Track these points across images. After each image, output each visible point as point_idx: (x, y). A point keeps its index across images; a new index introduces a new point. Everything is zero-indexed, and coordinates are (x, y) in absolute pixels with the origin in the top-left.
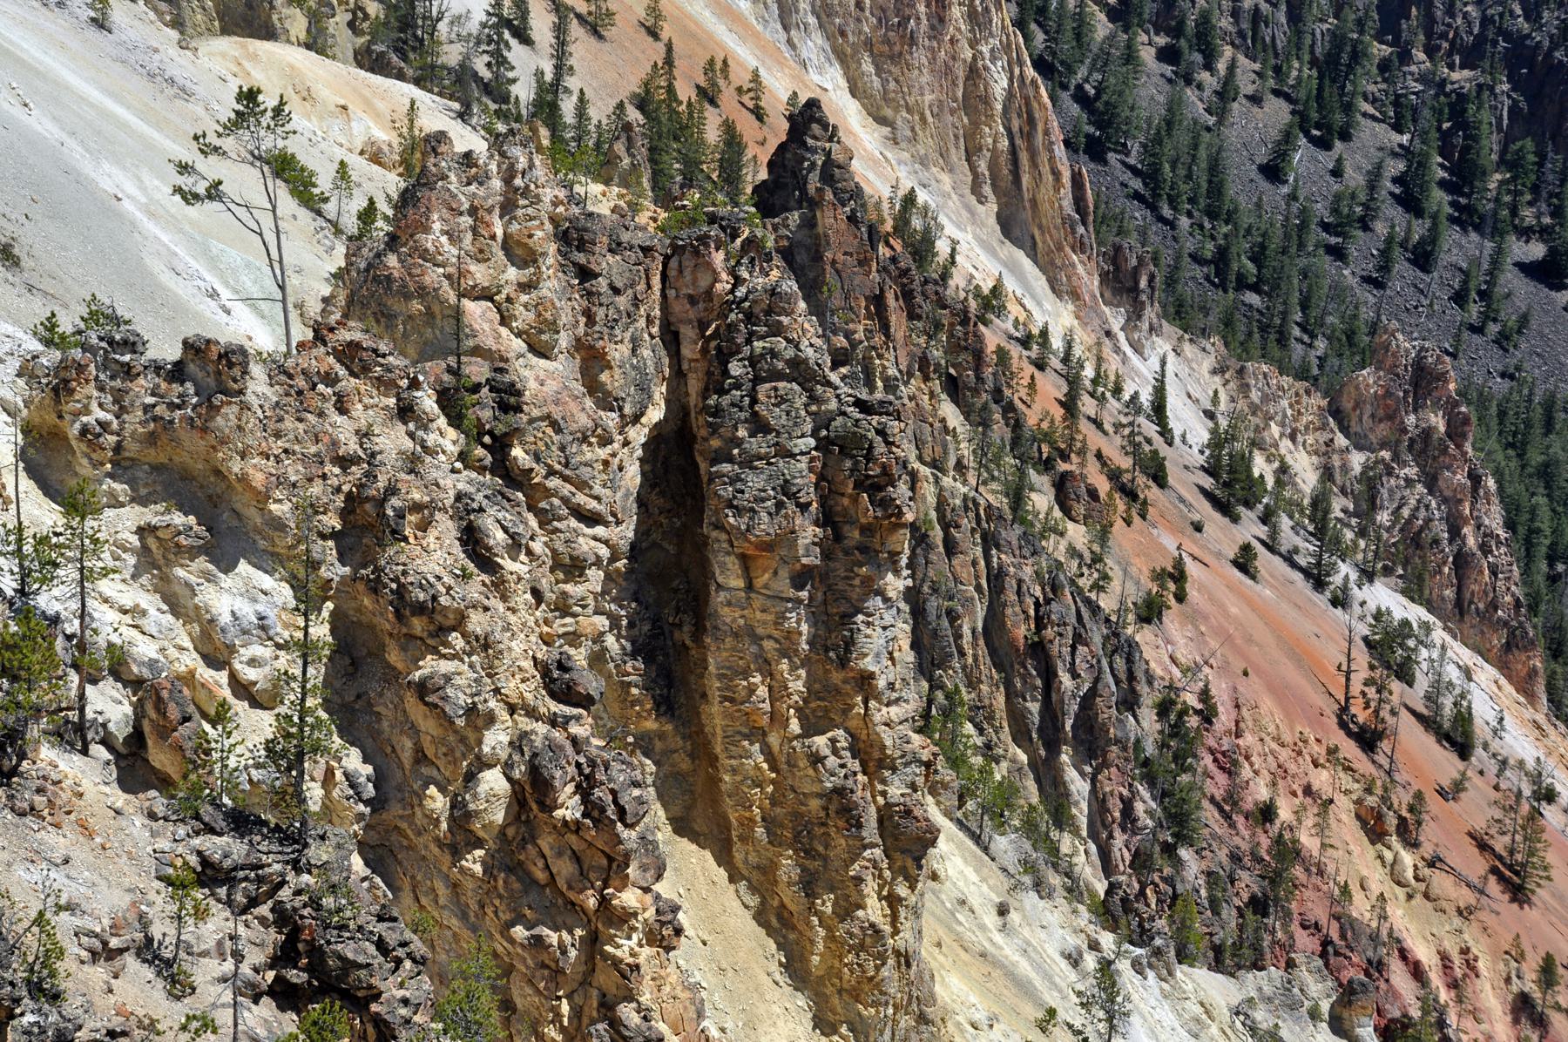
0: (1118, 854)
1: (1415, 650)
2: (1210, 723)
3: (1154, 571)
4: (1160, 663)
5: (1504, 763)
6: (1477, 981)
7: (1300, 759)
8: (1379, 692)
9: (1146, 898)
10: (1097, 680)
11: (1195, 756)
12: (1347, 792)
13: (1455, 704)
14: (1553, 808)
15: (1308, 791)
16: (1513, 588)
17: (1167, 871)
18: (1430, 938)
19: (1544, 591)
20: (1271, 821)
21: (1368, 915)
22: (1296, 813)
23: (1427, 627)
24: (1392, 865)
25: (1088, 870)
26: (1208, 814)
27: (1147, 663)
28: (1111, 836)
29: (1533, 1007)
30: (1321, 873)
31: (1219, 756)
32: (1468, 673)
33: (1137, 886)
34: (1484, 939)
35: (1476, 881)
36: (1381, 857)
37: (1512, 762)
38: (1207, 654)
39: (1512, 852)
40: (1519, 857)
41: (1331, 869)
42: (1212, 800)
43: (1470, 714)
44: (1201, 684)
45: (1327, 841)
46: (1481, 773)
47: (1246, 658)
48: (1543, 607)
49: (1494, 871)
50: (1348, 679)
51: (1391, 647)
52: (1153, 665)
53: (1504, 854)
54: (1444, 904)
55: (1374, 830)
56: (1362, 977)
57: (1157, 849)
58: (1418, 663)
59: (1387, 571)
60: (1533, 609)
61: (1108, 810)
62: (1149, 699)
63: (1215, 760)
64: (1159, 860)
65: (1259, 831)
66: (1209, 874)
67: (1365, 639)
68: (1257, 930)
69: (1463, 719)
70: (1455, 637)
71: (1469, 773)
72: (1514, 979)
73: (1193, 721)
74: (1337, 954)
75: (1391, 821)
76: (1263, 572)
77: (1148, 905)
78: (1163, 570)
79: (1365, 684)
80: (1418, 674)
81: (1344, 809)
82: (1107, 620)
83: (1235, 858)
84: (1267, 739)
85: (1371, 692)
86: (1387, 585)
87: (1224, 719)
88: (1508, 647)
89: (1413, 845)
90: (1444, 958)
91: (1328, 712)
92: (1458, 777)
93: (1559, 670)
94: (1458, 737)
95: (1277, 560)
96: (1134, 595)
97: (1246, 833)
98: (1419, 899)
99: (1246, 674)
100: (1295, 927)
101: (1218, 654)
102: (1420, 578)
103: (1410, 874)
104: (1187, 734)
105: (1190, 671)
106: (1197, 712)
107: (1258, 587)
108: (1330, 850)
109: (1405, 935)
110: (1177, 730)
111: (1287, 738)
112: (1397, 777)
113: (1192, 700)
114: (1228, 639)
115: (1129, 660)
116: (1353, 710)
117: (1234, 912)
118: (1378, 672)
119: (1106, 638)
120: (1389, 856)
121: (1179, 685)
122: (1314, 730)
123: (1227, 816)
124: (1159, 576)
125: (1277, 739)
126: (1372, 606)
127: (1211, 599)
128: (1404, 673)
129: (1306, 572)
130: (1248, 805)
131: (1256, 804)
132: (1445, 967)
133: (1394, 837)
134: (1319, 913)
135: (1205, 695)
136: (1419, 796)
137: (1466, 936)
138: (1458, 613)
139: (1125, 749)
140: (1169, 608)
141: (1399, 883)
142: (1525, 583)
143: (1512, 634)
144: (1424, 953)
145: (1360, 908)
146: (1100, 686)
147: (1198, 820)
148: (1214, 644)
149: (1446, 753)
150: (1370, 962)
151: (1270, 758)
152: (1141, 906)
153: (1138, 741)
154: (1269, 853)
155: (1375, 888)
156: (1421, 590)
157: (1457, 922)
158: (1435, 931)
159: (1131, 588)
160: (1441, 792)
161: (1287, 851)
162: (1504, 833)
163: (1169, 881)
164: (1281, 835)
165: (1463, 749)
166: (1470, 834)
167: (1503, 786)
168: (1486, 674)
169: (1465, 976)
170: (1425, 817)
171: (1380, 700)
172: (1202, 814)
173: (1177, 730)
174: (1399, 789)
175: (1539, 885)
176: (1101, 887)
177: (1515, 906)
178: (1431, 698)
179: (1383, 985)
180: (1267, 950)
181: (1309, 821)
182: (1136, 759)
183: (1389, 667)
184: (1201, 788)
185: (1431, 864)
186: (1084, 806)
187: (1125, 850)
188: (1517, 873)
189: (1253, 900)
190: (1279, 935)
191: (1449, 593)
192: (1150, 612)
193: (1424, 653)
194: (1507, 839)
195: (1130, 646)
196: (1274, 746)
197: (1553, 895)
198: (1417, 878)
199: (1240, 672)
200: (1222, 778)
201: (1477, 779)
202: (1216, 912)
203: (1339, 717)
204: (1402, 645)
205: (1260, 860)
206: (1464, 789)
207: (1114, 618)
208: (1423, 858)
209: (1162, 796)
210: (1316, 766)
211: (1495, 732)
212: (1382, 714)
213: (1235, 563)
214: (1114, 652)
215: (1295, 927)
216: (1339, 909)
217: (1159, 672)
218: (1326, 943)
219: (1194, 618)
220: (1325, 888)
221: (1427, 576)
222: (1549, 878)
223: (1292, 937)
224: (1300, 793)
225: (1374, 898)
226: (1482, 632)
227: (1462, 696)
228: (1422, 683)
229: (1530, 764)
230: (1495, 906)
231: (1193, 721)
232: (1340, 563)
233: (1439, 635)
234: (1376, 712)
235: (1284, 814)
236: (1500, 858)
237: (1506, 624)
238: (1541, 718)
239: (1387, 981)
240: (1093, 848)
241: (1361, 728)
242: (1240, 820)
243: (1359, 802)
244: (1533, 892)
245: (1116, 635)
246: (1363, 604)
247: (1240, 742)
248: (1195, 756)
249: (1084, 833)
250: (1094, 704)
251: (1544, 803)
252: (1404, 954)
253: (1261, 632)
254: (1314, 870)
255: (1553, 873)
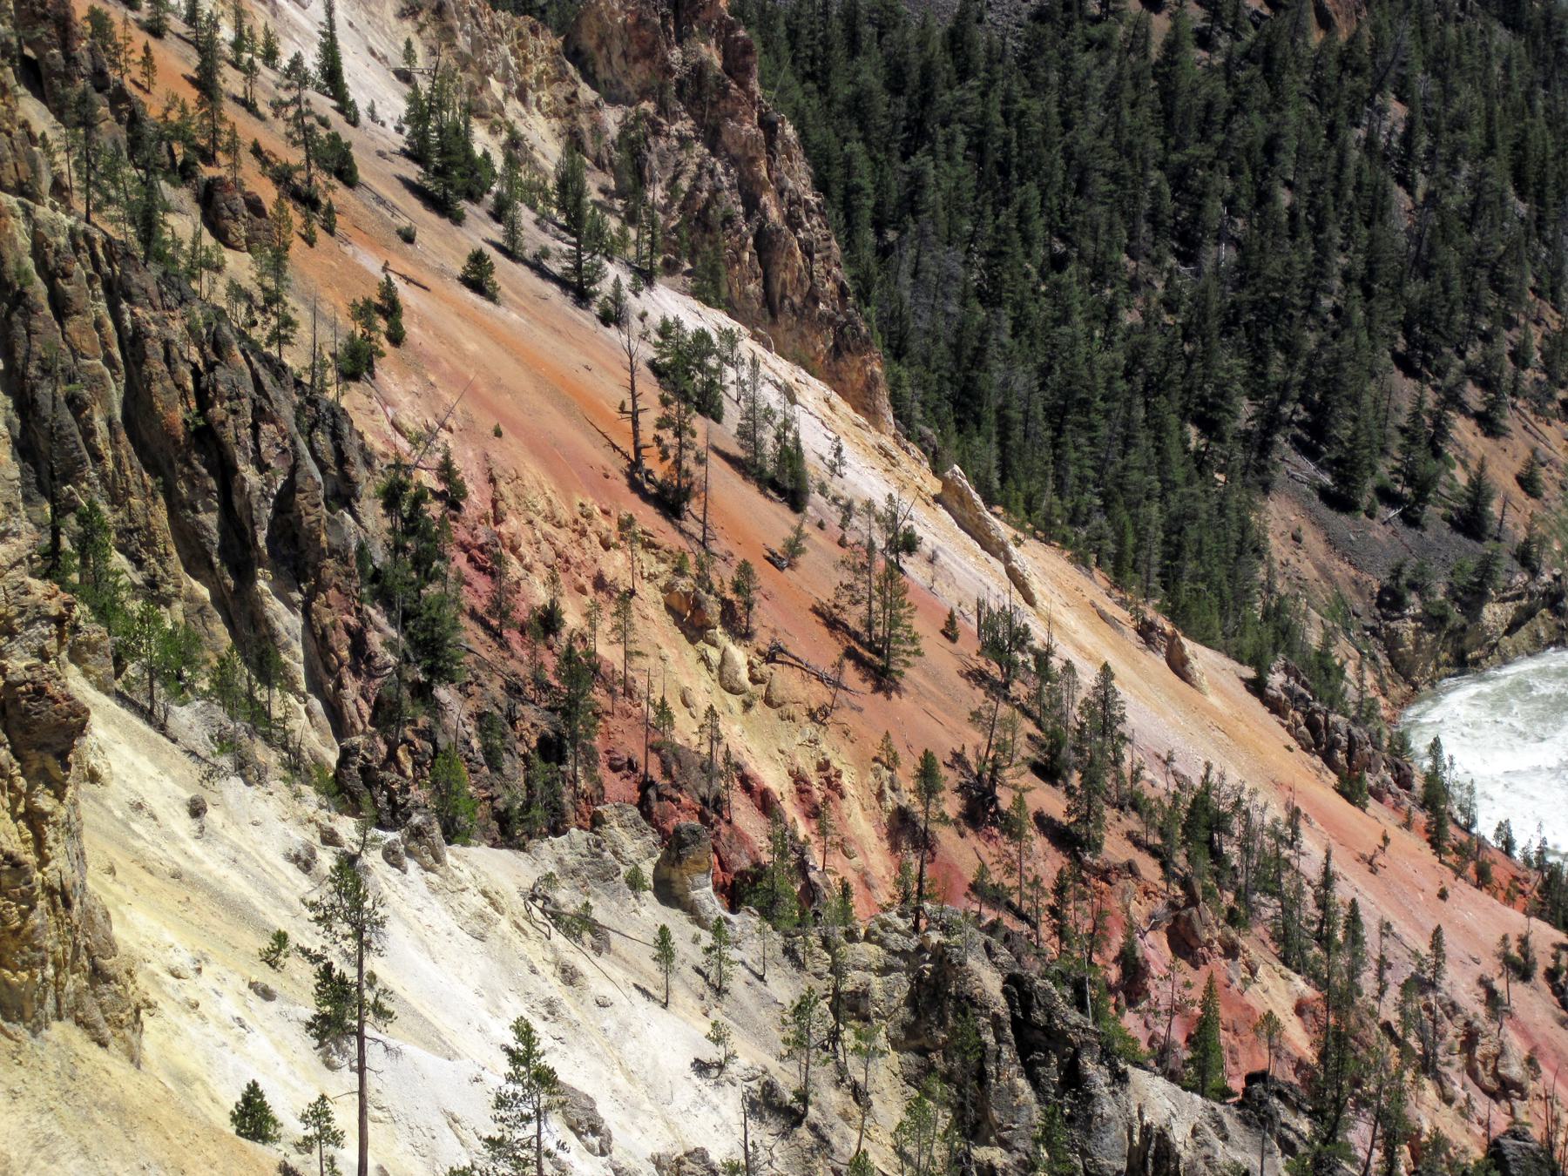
0: (353, 708)
1: (719, 371)
2: (457, 507)
3: (355, 305)
4: (379, 433)
5: (848, 508)
6: (844, 804)
7: (585, 542)
8: (678, 434)
9: (397, 762)
10: (294, 469)
11: (442, 557)
12: (652, 578)
13: (778, 438)
14: (914, 559)
15: (600, 583)
16: (835, 270)
17: (423, 721)
18: (778, 756)
19: (874, 269)
20: (556, 632)
21: (695, 739)
22: (587, 615)
23: (730, 338)
24: (721, 667)
25: (314, 736)
26: (470, 635)
27: (361, 436)
28: (340, 685)
29: (915, 824)
30: (629, 692)
31: (475, 552)
32: (789, 394)
33: (383, 748)
34: (846, 747)
35: (829, 671)
36: (704, 659)
37: (857, 505)
38: (442, 413)
39: (869, 626)
40: (879, 631)
41: (641, 684)
42: (473, 614)
43: (798, 448)
44: (439, 456)
45: (632, 648)
46: (821, 525)
47: (495, 411)
48: (875, 292)
49: (850, 654)
50: (635, 423)
51: (687, 372)
52: (369, 437)
53: (861, 630)
54: (792, 709)
55: (693, 626)
56: (696, 823)
57: (406, 693)
58: (724, 389)
59: (670, 268)
60: (864, 296)
61: (332, 650)
62: (369, 485)
63: (471, 559)
64: (409, 707)
65: (541, 647)
66: (480, 717)
67: (652, 365)
68: (550, 784)
69: (791, 457)
70: (768, 347)
71: (806, 529)
72: (888, 792)
73: (434, 509)
74: (660, 797)
75: (713, 608)
76: (504, 288)
77: (402, 773)
78: (368, 302)
79: (659, 427)
80: (727, 405)
81: (649, 599)
82: (298, 383)
83: (513, 690)
84: (538, 520)
85: (668, 436)
86: (672, 287)
87: (476, 499)
88: (837, 351)
89: (743, 635)
90: (799, 779)
91: (614, 471)
92: (792, 535)
93: (904, 374)
94: (786, 482)
95: (521, 271)
96: (332, 343)
97: (523, 654)
98: (759, 705)
99: (498, 433)
100: (603, 771)
101: (458, 411)
102: (714, 273)
103: (744, 675)
104: (427, 529)
105: (422, 439)
106: (439, 496)
107: (501, 311)
108: (638, 660)
109: (746, 758)
110: (413, 525)
111: (564, 514)
112: (714, 547)
113: (429, 480)
114: (468, 389)
115: (336, 436)
116: (647, 464)
117: (519, 763)
118: (674, 407)
119: (299, 410)
120: (714, 655)
121: (410, 461)
122: (598, 499)
123: (496, 634)
124: (363, 312)
125: (551, 518)
126: (655, 319)
127: (440, 336)
128: (708, 405)
129: (562, 282)
130: (522, 614)
131: (533, 611)
132: (800, 791)
133: (719, 629)
134: (632, 746)
135: (446, 471)
136: (745, 569)
137: (824, 747)
138: (767, 312)
139: (344, 561)
140: (382, 355)
141: (731, 690)
142: (849, 262)
143: (839, 333)
144: (773, 778)
145: (685, 731)
146: (299, 478)
147: (457, 645)
148: (449, 397)
149: (773, 506)
150: (704, 801)
151: (545, 546)
152: (391, 776)
153: (362, 548)
154: (557, 675)
155: (701, 701)
156: (716, 288)
157: (810, 729)
158: (783, 746)
159: (325, 334)
160: (773, 559)
161: (581, 669)
162: (857, 602)
163: (428, 734)
164: (570, 649)
165: (795, 498)
166: (815, 610)
167: (850, 539)
168: (813, 391)
169: (826, 798)
170: (756, 595)
171: (681, 446)
172: (462, 636)
173: (413, 525)
174: (719, 564)
175: (907, 664)
176: (332, 757)
177: (880, 696)
178: (747, 434)
179: (724, 829)
180: (569, 807)
181: (605, 626)
182: (362, 572)
183: (687, 399)
184: (456, 601)
185: (770, 658)
186: (298, 648)
187: (361, 702)
188: (879, 653)
189: (544, 742)
190: (583, 784)
191: (753, 287)
192: (357, 364)
193: (731, 374)
194: (862, 609)
195: (334, 415)
196: (548, 528)
197: (926, 674)
198: (754, 680)
199: (490, 433)
200: (482, 583)
201: (816, 536)
202: (495, 767)
203: (630, 476)
204: (701, 367)
205: (544, 687)
206: (802, 551)
207: (306, 379)
208: (759, 652)
209: (404, 618)
210: (607, 548)
211: (833, 468)
212: (685, 464)
213: (466, 281)
214: (313, 426)
215: (603, 771)
216: (658, 737)
217: (379, 446)
218: (645, 785)
219: (418, 364)
220: (636, 711)
221: (722, 268)
222: (918, 653)
223: (600, 786)
224: (589, 587)
225: (701, 714)
226: (802, 336)
227: (786, 425)
228: (733, 415)
229: (881, 505)
230: (855, 701)
231: (434, 509)
232: (607, 264)
233: (747, 346)
234: (678, 462)
235: (572, 619)
236: (856, 636)
237: (831, 320)
238: (888, 442)
239: (729, 822)
240: (317, 705)
241: (659, 487)
242: (513, 637)
243: (668, 589)
244: (901, 674)
245: (313, 402)
246: (643, 316)
247: (502, 529)
248: (442, 557)
249: (303, 687)
250: (293, 503)
251: (903, 555)
252: (747, 784)
253: (510, 371)
254: (619, 689)
255: (923, 645)
